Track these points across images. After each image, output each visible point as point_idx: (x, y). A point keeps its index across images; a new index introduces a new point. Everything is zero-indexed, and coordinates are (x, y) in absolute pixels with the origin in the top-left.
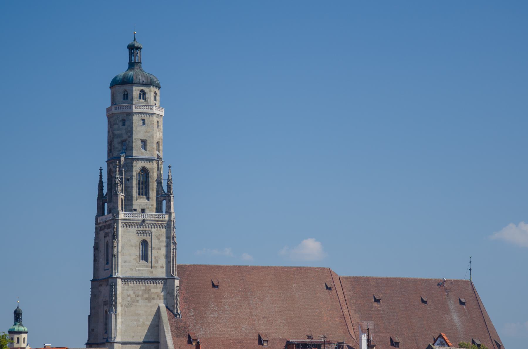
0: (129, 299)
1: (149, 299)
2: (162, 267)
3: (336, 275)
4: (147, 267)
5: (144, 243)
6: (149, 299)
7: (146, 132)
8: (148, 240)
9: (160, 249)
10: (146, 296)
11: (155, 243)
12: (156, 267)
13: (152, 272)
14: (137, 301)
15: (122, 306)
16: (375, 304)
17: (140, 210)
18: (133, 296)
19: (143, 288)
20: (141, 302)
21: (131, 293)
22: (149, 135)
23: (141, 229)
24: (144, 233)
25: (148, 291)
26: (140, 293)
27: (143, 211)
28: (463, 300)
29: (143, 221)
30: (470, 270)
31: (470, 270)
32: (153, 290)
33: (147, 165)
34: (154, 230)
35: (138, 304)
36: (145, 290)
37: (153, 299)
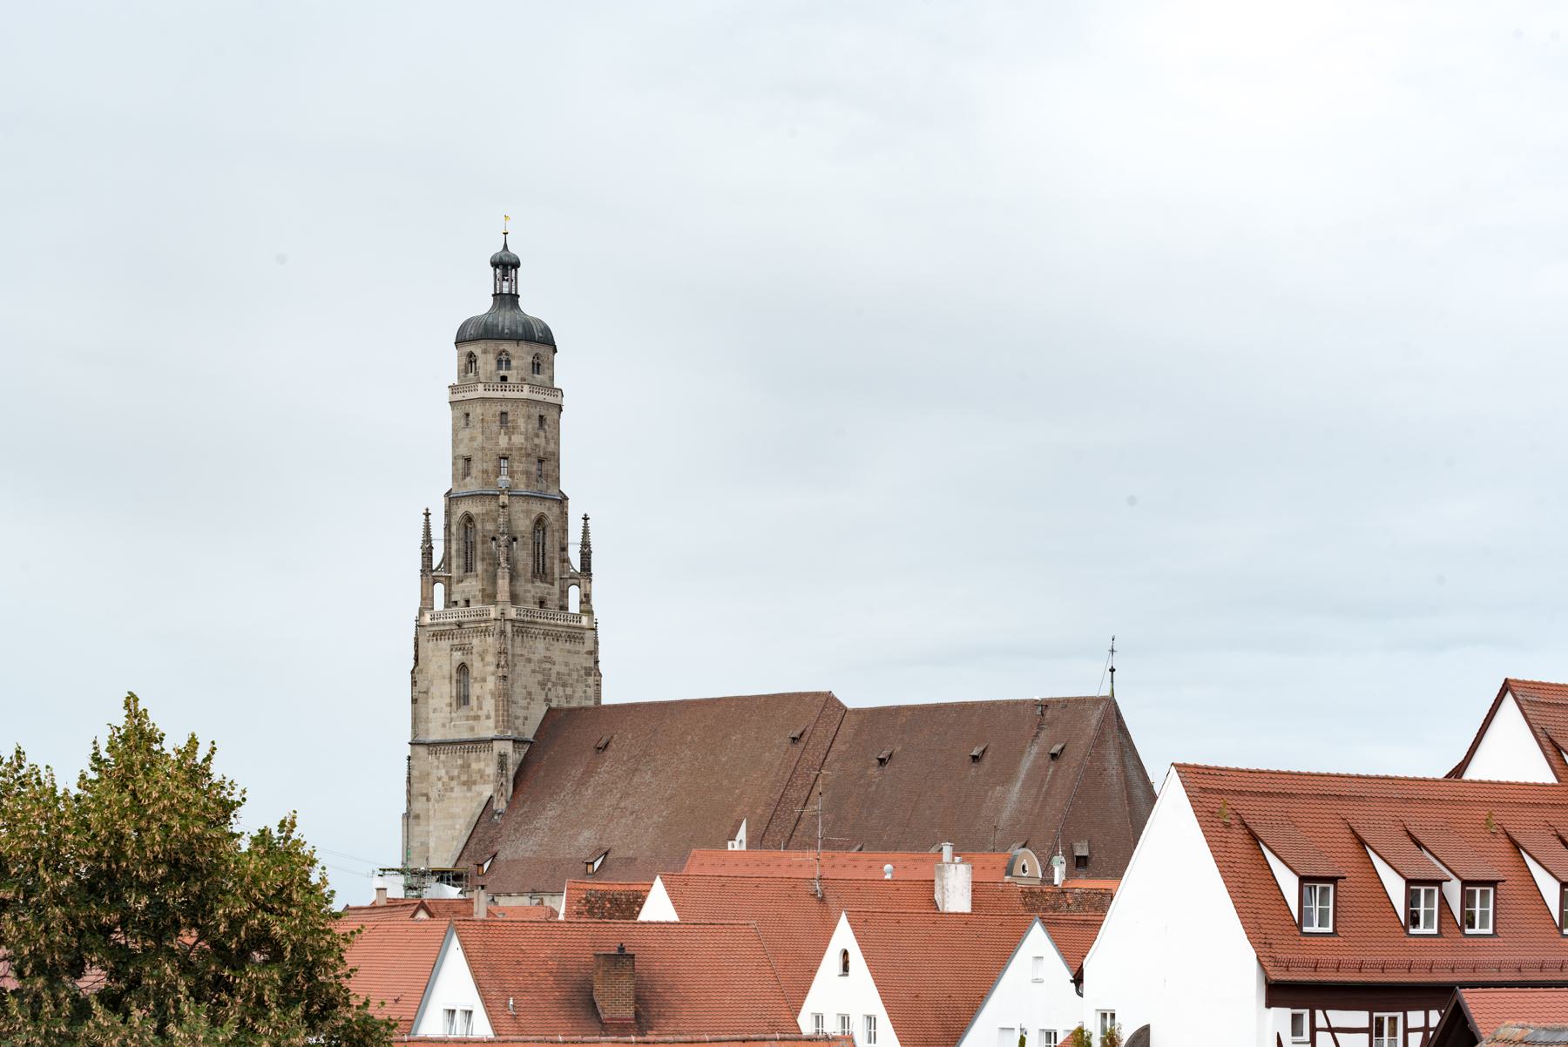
0: (440, 784)
1: (469, 784)
2: (488, 717)
3: (840, 704)
4: (468, 718)
5: (463, 668)
6: (469, 784)
7: (472, 439)
8: (468, 663)
9: (484, 680)
10: (464, 778)
11: (476, 668)
12: (477, 718)
13: (472, 729)
14: (452, 789)
15: (428, 800)
16: (874, 771)
17: (462, 603)
18: (445, 779)
19: (460, 762)
20: (458, 791)
21: (442, 772)
22: (475, 444)
23: (456, 642)
24: (461, 648)
25: (466, 767)
26: (456, 773)
27: (467, 602)
28: (1056, 749)
29: (460, 625)
30: (1112, 670)
31: (1112, 670)
32: (474, 766)
33: (474, 508)
34: (475, 642)
35: (453, 795)
36: (462, 767)
37: (475, 783)
